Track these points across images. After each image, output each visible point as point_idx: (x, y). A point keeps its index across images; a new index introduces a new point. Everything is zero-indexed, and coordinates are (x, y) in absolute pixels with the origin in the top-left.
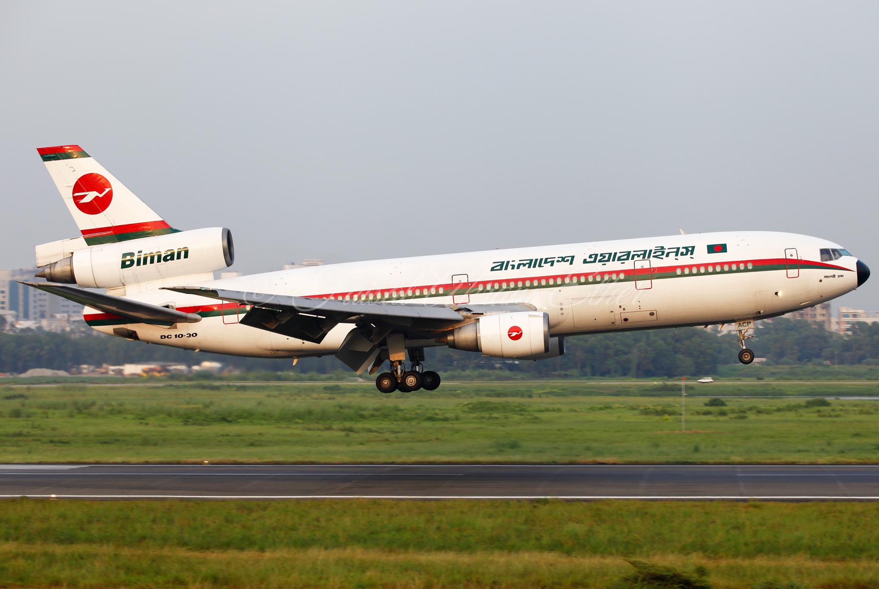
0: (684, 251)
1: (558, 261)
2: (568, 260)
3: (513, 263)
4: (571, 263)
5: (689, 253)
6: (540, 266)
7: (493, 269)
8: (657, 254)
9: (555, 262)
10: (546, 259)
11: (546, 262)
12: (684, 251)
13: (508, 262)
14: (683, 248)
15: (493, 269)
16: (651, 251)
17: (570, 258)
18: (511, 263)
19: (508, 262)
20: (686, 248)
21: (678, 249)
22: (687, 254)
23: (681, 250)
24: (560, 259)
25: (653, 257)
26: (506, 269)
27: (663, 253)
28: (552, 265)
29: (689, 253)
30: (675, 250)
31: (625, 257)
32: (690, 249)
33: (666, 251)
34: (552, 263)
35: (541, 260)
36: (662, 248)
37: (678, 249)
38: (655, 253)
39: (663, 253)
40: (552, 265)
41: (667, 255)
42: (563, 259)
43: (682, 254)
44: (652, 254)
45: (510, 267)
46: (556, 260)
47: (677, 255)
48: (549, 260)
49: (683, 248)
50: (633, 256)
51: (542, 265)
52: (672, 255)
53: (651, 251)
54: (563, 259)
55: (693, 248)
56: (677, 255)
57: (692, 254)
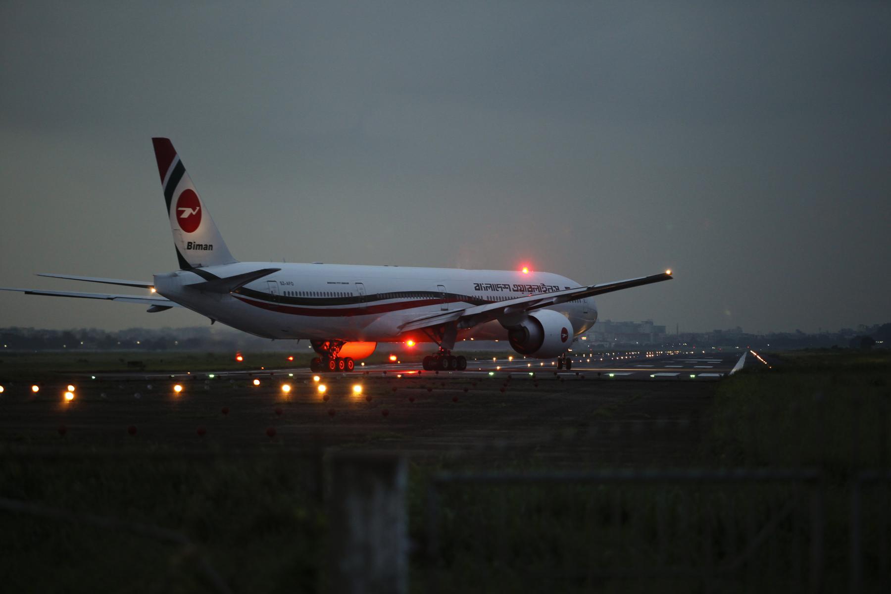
2: (507, 288)
4: (510, 291)
8: (545, 289)
10: (497, 285)
11: (498, 288)
15: (476, 289)
18: (482, 285)
23: (554, 288)
27: (546, 288)
28: (502, 290)
33: (547, 287)
40: (502, 290)
44: (542, 290)
45: (483, 288)
48: (499, 286)
51: (498, 289)
52: (551, 291)
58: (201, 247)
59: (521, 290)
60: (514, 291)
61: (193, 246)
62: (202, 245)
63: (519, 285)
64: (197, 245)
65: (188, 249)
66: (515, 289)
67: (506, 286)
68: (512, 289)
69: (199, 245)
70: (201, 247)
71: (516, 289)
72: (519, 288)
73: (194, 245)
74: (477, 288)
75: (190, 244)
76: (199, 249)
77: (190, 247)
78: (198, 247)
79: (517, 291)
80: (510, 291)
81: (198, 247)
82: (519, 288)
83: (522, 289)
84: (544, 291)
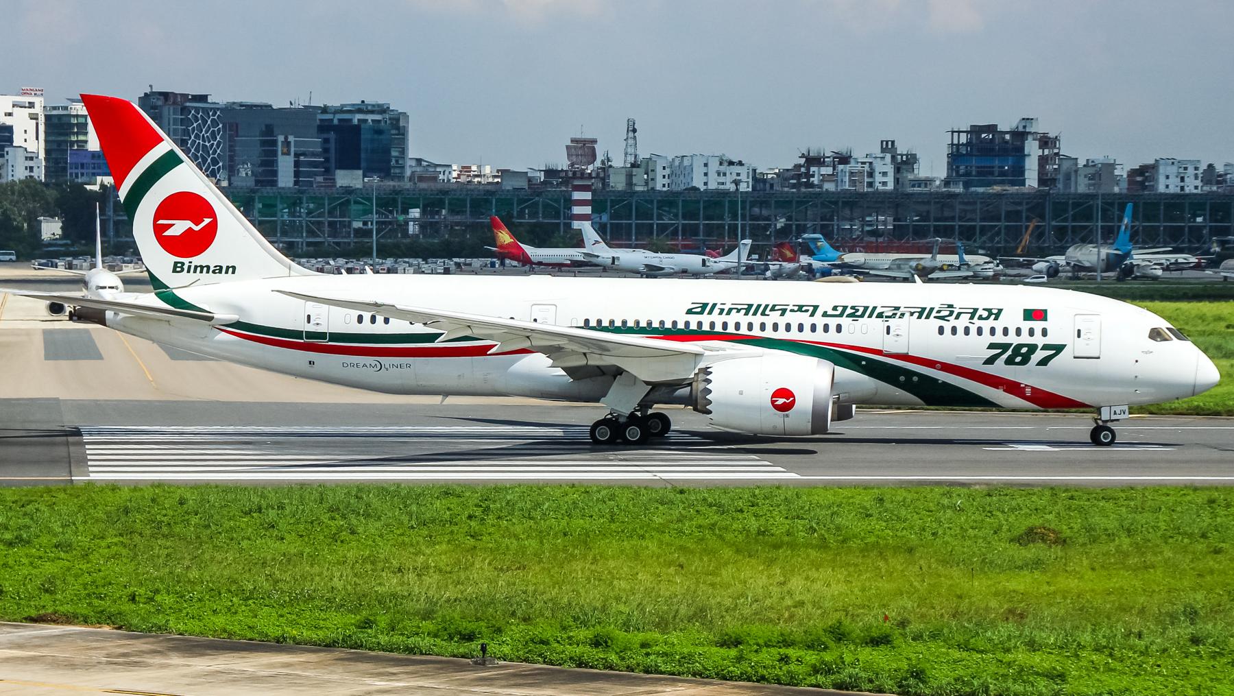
0: (985, 314)
1: (792, 311)
2: (807, 311)
3: (722, 307)
4: (812, 315)
5: (993, 316)
6: (763, 314)
7: (690, 312)
8: (943, 314)
9: (788, 311)
10: (774, 306)
11: (773, 309)
12: (985, 314)
13: (714, 305)
14: (984, 309)
15: (690, 312)
16: (932, 309)
17: (811, 309)
18: (719, 306)
19: (714, 305)
20: (989, 311)
21: (976, 310)
22: (987, 318)
23: (979, 313)
24: (796, 308)
25: (935, 317)
26: (710, 313)
28: (782, 315)
29: (993, 316)
30: (972, 311)
31: (890, 314)
32: (995, 311)
34: (783, 312)
35: (767, 306)
36: (951, 306)
37: (976, 310)
38: (939, 312)
39: (951, 313)
40: (782, 315)
41: (957, 318)
42: (801, 308)
43: (980, 318)
44: (934, 314)
45: (716, 311)
46: (789, 308)
47: (972, 318)
48: (777, 308)
49: (984, 309)
50: (903, 315)
52: (965, 319)
53: (932, 309)
54: (801, 308)
55: (1000, 311)
56: (972, 318)
57: (996, 319)
58: (205, 269)
59: (848, 316)
60: (825, 315)
61: (186, 267)
62: (208, 267)
63: (853, 308)
64: (196, 267)
65: (174, 271)
66: (830, 312)
67: (804, 309)
68: (819, 312)
69: (202, 267)
70: (205, 269)
71: (838, 313)
72: (849, 311)
73: (189, 267)
74: (699, 310)
75: (179, 265)
76: (201, 272)
77: (178, 269)
78: (199, 269)
79: (841, 315)
80: (812, 315)
81: (199, 269)
82: (849, 311)
83: (859, 313)
84: (935, 317)
